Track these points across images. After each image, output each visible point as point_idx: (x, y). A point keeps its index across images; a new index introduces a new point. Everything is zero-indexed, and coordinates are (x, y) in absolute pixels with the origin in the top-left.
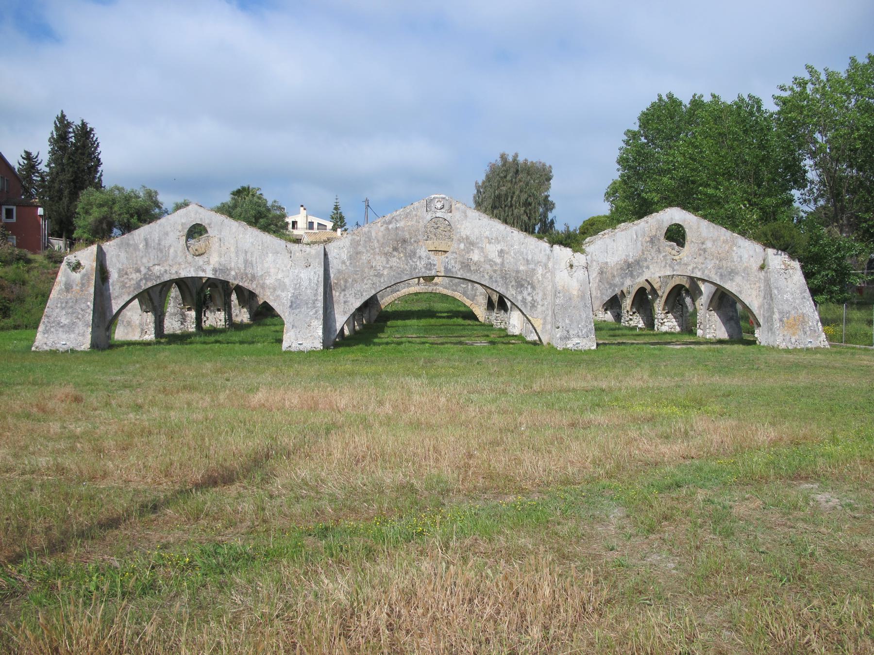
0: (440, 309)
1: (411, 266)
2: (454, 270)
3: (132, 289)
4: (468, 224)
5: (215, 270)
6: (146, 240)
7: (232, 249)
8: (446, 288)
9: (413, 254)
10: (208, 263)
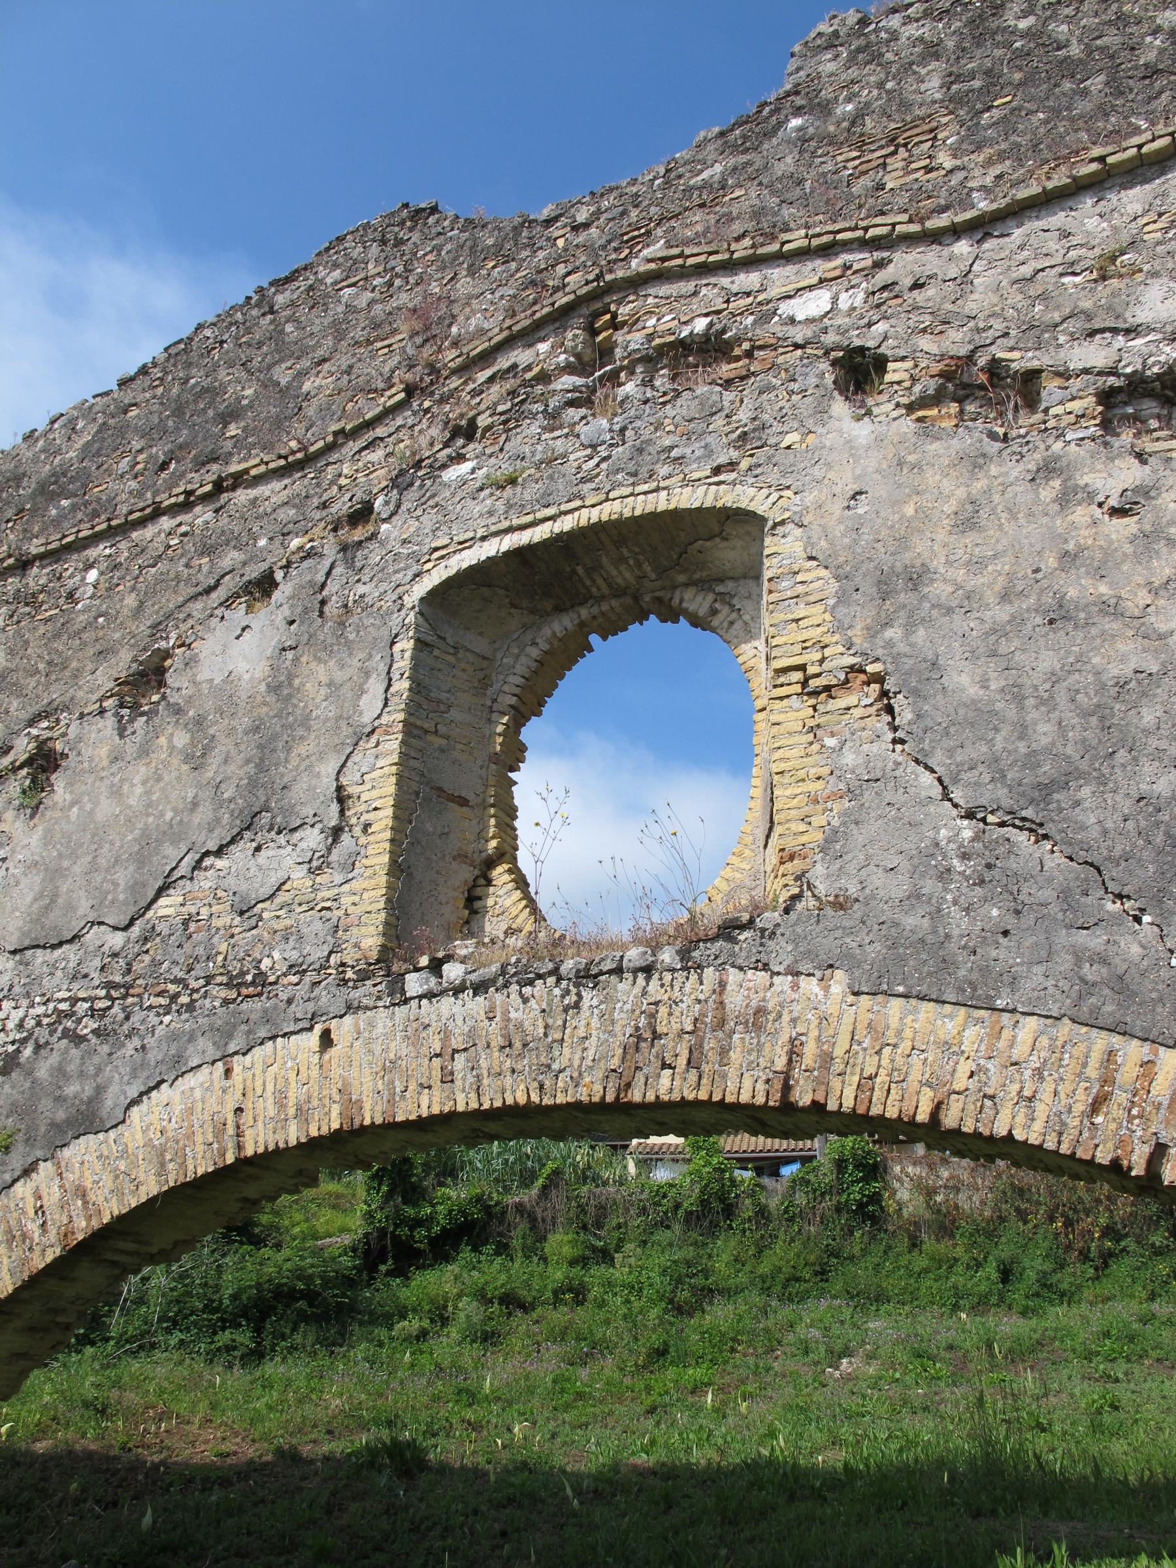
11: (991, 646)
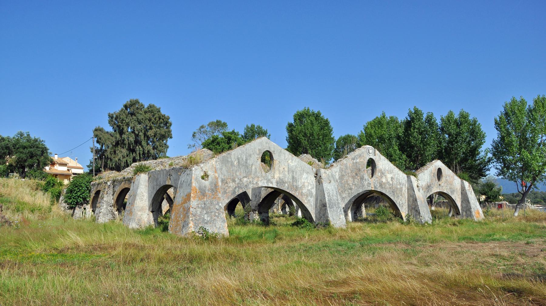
3: (230, 194)
5: (277, 183)
6: (238, 159)
7: (286, 169)
10: (274, 177)
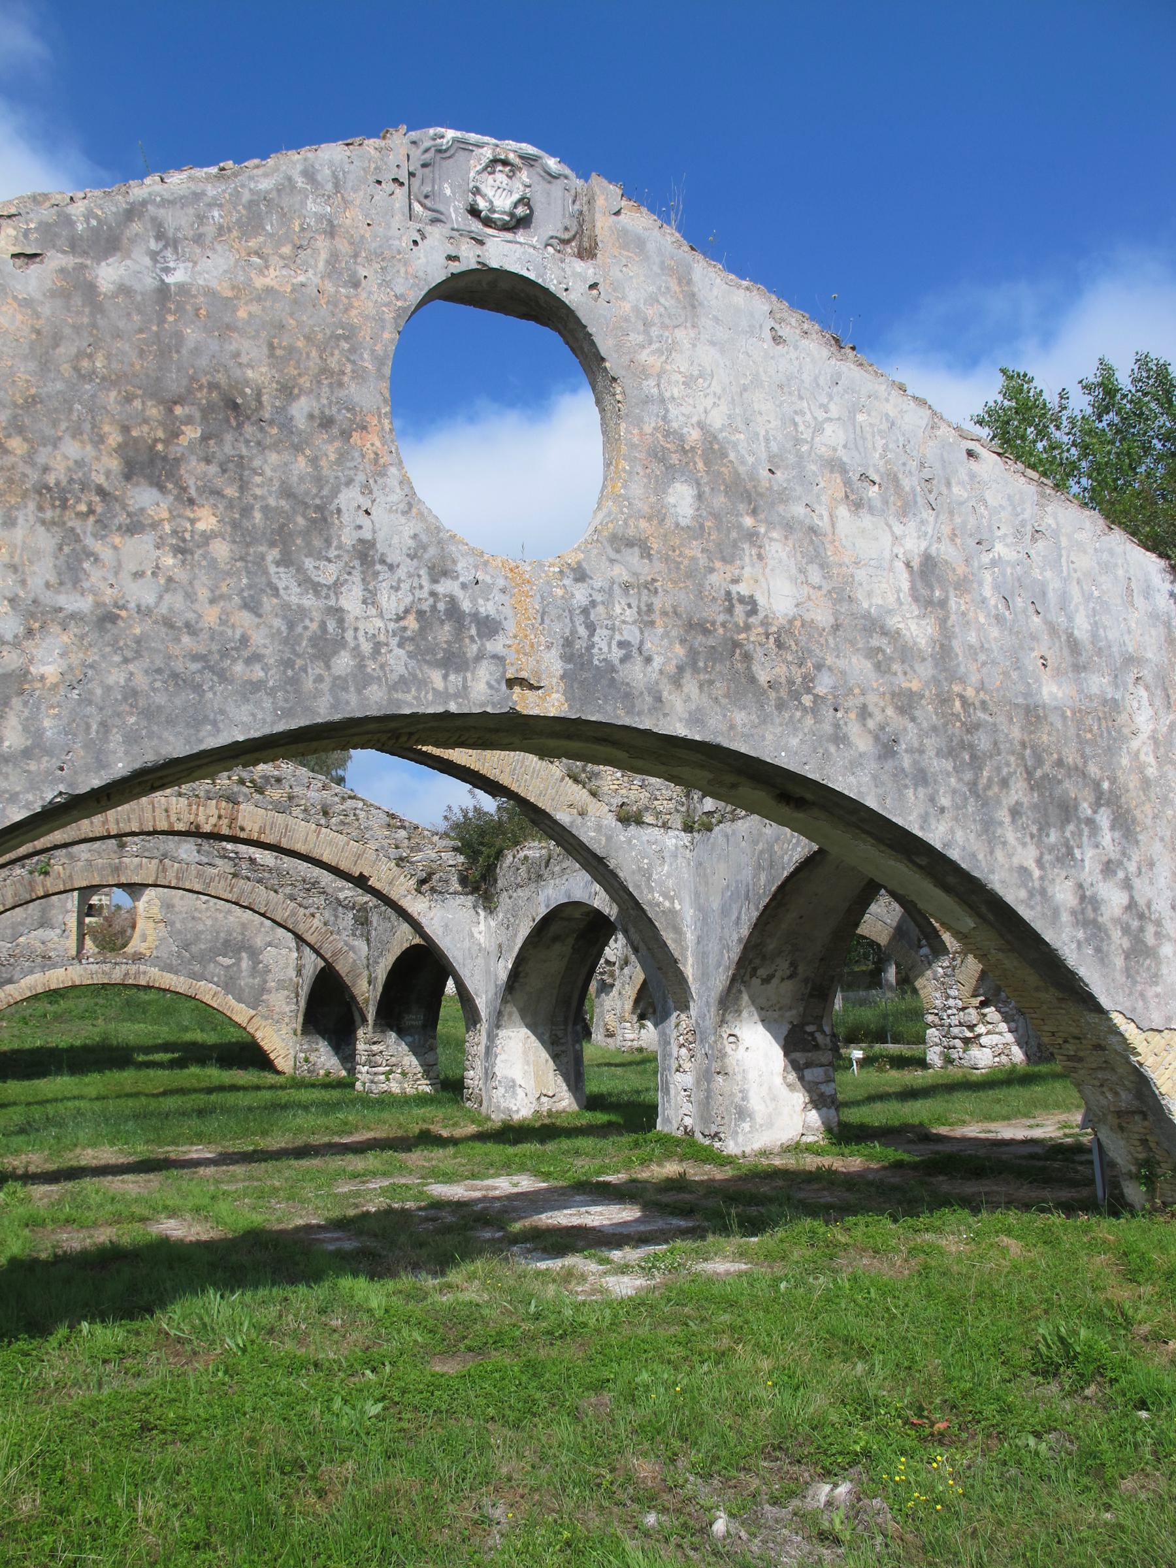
0: (132, 1039)
1: (294, 617)
2: (636, 674)
4: (707, 356)
8: (168, 968)
9: (303, 525)
11: (183, 921)
